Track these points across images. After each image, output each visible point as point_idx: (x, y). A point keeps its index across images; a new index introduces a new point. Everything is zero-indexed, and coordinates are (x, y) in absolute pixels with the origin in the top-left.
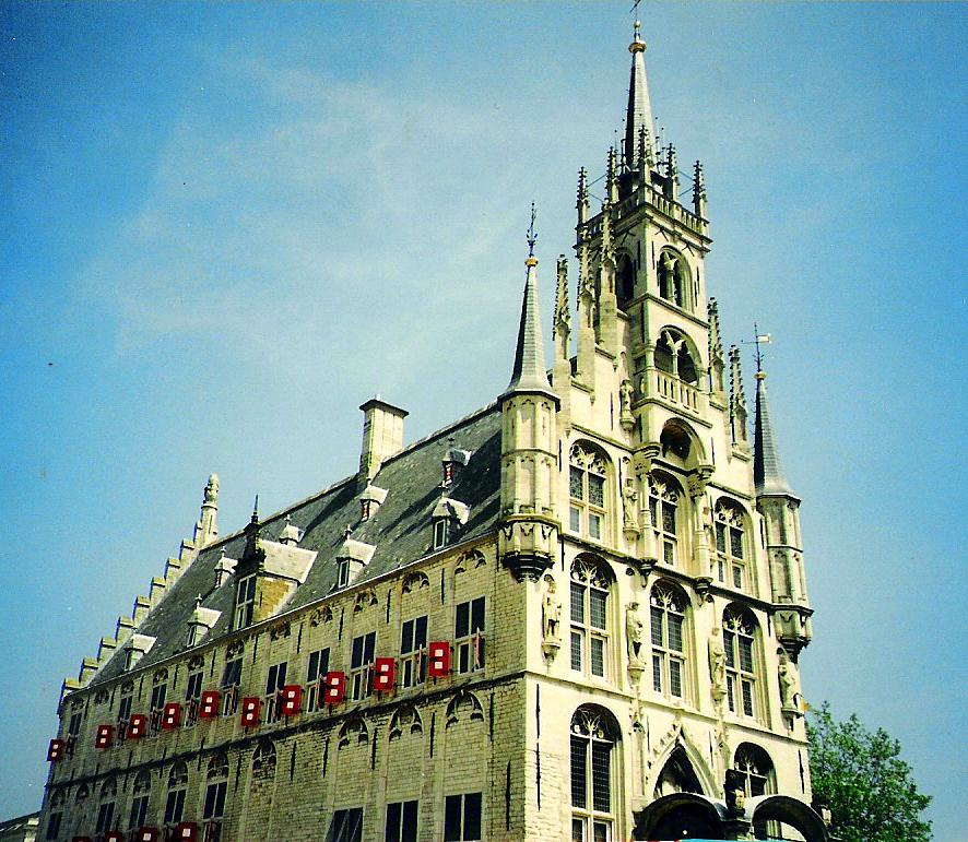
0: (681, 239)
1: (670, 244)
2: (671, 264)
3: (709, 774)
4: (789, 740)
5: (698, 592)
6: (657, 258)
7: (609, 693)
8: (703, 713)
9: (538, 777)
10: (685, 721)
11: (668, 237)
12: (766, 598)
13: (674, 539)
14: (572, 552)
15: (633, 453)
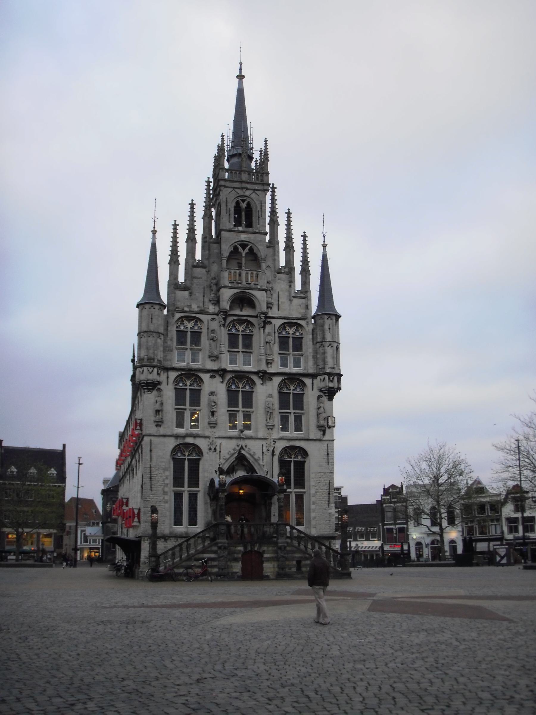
0: (247, 189)
1: (242, 194)
2: (244, 205)
3: (259, 464)
4: (320, 440)
5: (260, 377)
6: (232, 206)
7: (195, 436)
8: (260, 435)
9: (151, 478)
10: (242, 443)
11: (239, 191)
13: (251, 352)
14: (173, 375)
15: (218, 315)
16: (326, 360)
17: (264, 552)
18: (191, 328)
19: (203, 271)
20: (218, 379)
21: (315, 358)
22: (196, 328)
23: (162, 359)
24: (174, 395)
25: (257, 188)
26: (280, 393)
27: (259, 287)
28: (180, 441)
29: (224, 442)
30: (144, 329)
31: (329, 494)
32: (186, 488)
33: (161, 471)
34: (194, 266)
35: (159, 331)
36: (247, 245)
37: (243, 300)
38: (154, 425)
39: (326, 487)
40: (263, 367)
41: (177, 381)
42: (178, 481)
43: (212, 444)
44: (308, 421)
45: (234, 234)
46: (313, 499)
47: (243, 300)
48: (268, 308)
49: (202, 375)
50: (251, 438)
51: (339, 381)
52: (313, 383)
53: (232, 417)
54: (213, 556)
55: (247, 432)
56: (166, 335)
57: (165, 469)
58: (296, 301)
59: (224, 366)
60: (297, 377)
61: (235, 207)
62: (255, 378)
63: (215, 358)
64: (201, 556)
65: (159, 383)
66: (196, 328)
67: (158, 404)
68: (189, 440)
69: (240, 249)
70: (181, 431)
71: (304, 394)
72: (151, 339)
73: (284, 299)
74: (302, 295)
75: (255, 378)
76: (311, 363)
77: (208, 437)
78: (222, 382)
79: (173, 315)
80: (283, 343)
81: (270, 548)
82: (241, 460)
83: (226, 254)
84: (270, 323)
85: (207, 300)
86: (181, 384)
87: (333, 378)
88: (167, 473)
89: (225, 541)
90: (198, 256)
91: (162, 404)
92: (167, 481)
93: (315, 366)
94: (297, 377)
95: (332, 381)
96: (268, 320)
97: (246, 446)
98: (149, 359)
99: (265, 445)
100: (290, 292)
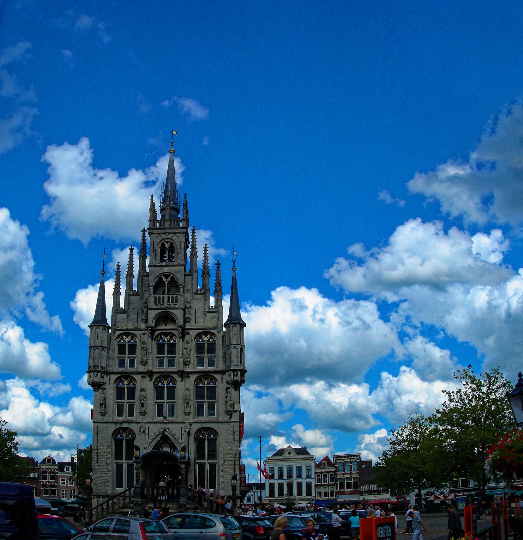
0: (169, 233)
1: (166, 237)
2: (167, 246)
4: (227, 422)
8: (179, 420)
9: (97, 454)
10: (166, 426)
12: (221, 367)
14: (114, 377)
15: (147, 330)
16: (232, 359)
17: (169, 508)
18: (128, 341)
19: (138, 298)
20: (147, 379)
21: (224, 358)
22: (133, 341)
23: (105, 366)
24: (115, 392)
25: (177, 231)
27: (177, 306)
28: (118, 426)
29: (151, 426)
30: (93, 345)
31: (235, 464)
32: (124, 461)
33: (105, 448)
34: (130, 295)
35: (104, 345)
36: (169, 276)
37: (165, 317)
38: (99, 415)
39: (233, 459)
40: (181, 367)
42: (118, 455)
43: (141, 427)
45: (159, 268)
46: (221, 468)
48: (186, 321)
49: (134, 376)
50: (172, 422)
52: (222, 378)
53: (160, 407)
55: (170, 418)
56: (109, 348)
57: (108, 447)
58: (209, 315)
59: (150, 368)
60: (209, 374)
61: (161, 248)
62: (175, 376)
63: (144, 363)
64: (122, 510)
65: (104, 384)
66: (133, 341)
67: (102, 398)
68: (125, 425)
70: (121, 418)
71: (216, 387)
72: (96, 351)
73: (199, 314)
74: (215, 310)
75: (175, 376)
76: (221, 362)
77: (140, 423)
78: (150, 381)
79: (115, 333)
80: (200, 348)
81: (174, 506)
82: (165, 439)
83: (153, 284)
84: (188, 333)
85: (140, 319)
86: (121, 384)
87: (237, 374)
88: (109, 450)
89: (140, 500)
91: (105, 399)
92: (109, 456)
93: (224, 365)
94: (209, 374)
95: (236, 376)
96: (187, 331)
97: (168, 429)
98: (94, 366)
99: (183, 427)
100: (205, 308)
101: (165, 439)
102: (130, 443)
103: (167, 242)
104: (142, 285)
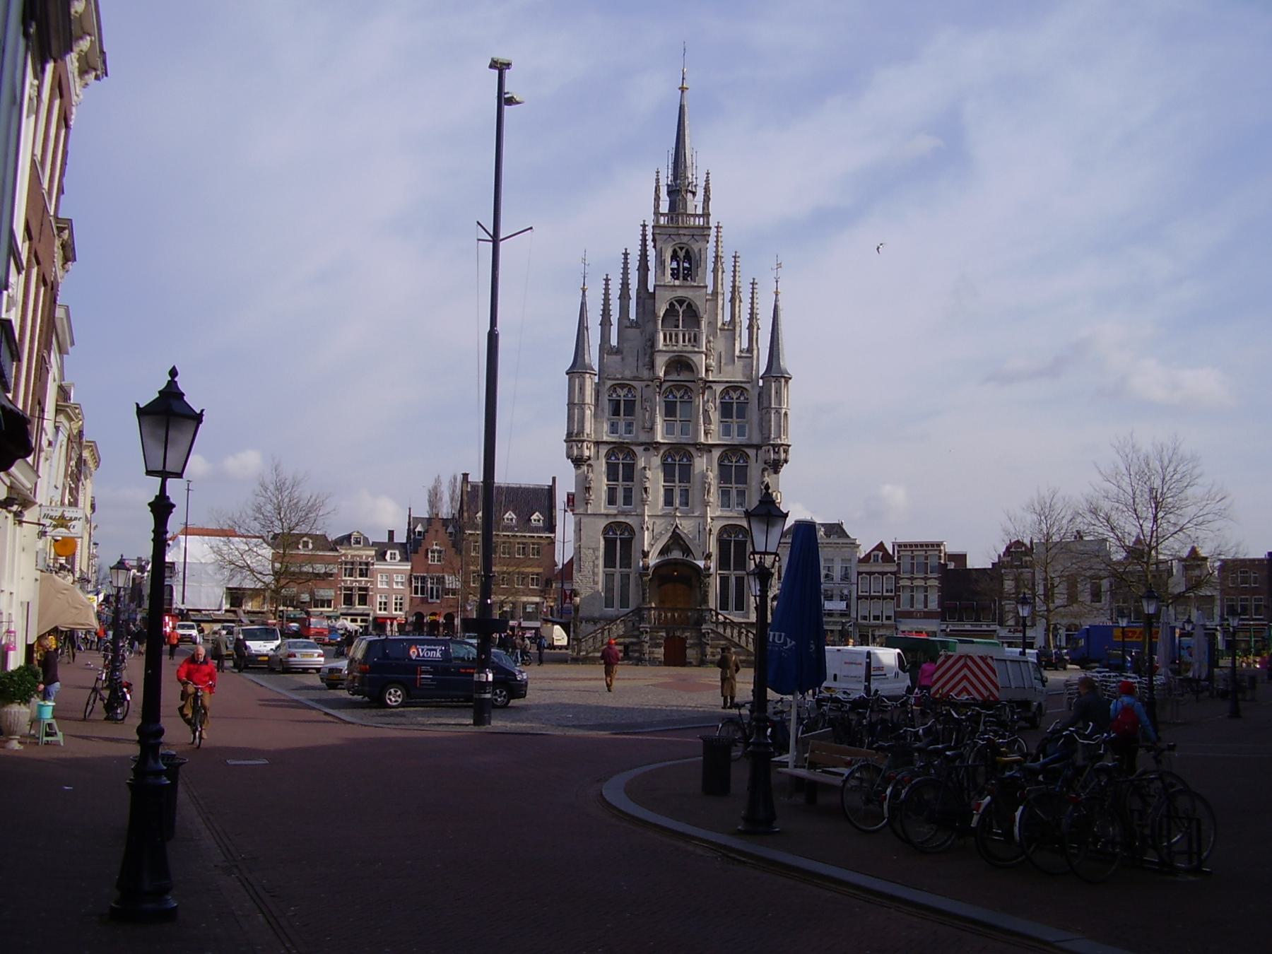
2: (682, 254)
12: (756, 439)
14: (604, 450)
26: (720, 465)
41: (608, 456)
42: (609, 561)
44: (750, 496)
47: (680, 364)
48: (707, 371)
51: (786, 452)
54: (634, 640)
62: (692, 450)
65: (589, 458)
69: (677, 306)
75: (692, 450)
80: (726, 410)
84: (710, 387)
85: (640, 364)
90: (633, 316)
101: (677, 540)
102: (627, 544)
103: (681, 249)
104: (644, 313)
